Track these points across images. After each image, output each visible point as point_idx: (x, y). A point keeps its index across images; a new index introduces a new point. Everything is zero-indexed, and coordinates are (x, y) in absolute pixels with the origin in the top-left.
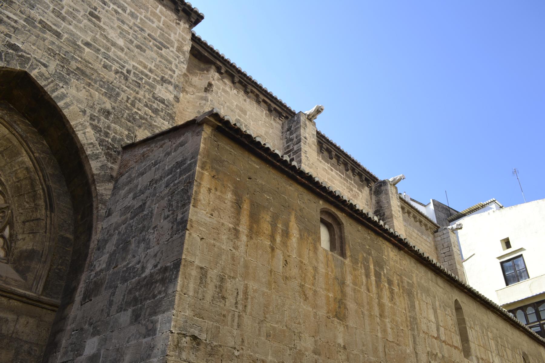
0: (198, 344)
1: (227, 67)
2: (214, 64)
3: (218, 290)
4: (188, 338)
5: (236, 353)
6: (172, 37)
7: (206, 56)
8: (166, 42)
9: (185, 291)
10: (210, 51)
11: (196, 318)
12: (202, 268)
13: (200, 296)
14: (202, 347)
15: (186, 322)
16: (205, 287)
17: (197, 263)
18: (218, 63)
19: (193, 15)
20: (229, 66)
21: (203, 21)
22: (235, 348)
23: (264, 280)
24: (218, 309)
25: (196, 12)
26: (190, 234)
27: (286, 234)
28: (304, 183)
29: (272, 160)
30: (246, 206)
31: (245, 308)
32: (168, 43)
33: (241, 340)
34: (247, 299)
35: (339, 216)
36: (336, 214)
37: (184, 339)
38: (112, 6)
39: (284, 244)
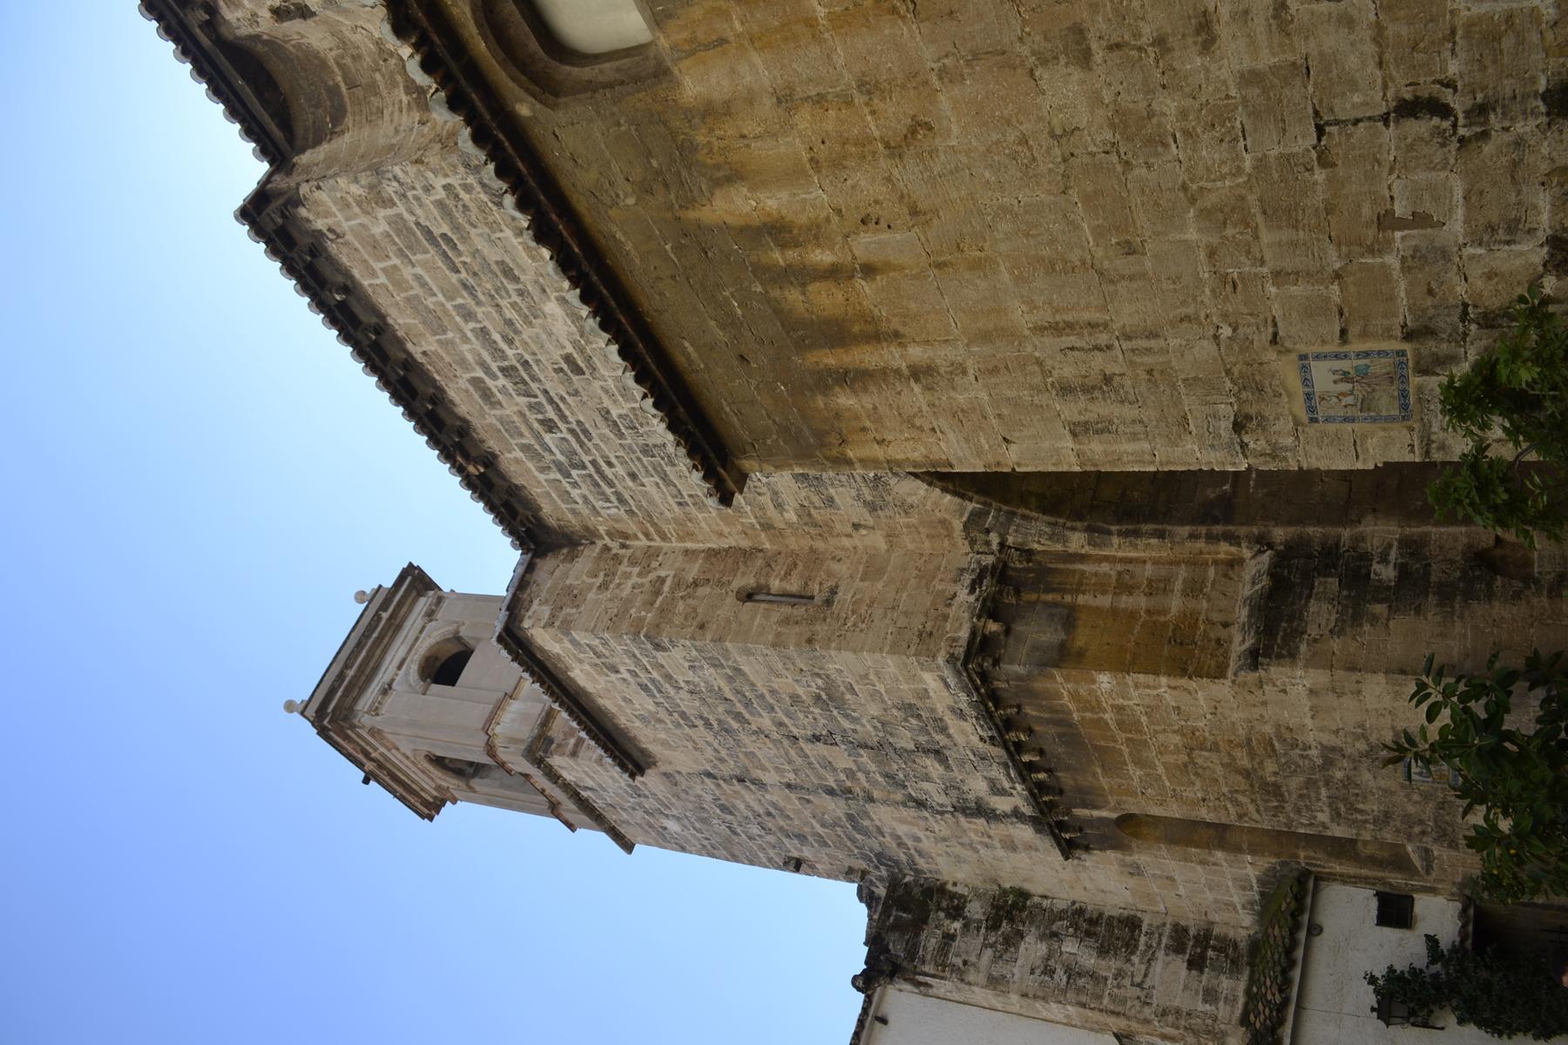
0: (1248, 418)
1: (176, 15)
2: (219, 41)
3: (1097, 394)
4: (1246, 439)
5: (1226, 331)
6: (380, 228)
7: (243, 78)
8: (417, 239)
9: (1147, 458)
10: (223, 87)
11: (1192, 427)
12: (1074, 434)
13: (1138, 428)
14: (1253, 411)
15: (1212, 446)
16: (1111, 422)
17: (1068, 443)
18: (205, 41)
19: (300, 266)
20: (169, 16)
21: (239, 203)
22: (1216, 337)
23: (982, 284)
24: (1143, 388)
25: (259, 231)
26: (1019, 465)
27: (777, 231)
28: (559, 216)
29: (636, 339)
30: (830, 359)
31: (1098, 325)
32: (409, 230)
33: (1185, 324)
34: (1070, 326)
35: (467, 10)
36: (479, 25)
37: (1252, 445)
38: (510, 352)
39: (816, 233)
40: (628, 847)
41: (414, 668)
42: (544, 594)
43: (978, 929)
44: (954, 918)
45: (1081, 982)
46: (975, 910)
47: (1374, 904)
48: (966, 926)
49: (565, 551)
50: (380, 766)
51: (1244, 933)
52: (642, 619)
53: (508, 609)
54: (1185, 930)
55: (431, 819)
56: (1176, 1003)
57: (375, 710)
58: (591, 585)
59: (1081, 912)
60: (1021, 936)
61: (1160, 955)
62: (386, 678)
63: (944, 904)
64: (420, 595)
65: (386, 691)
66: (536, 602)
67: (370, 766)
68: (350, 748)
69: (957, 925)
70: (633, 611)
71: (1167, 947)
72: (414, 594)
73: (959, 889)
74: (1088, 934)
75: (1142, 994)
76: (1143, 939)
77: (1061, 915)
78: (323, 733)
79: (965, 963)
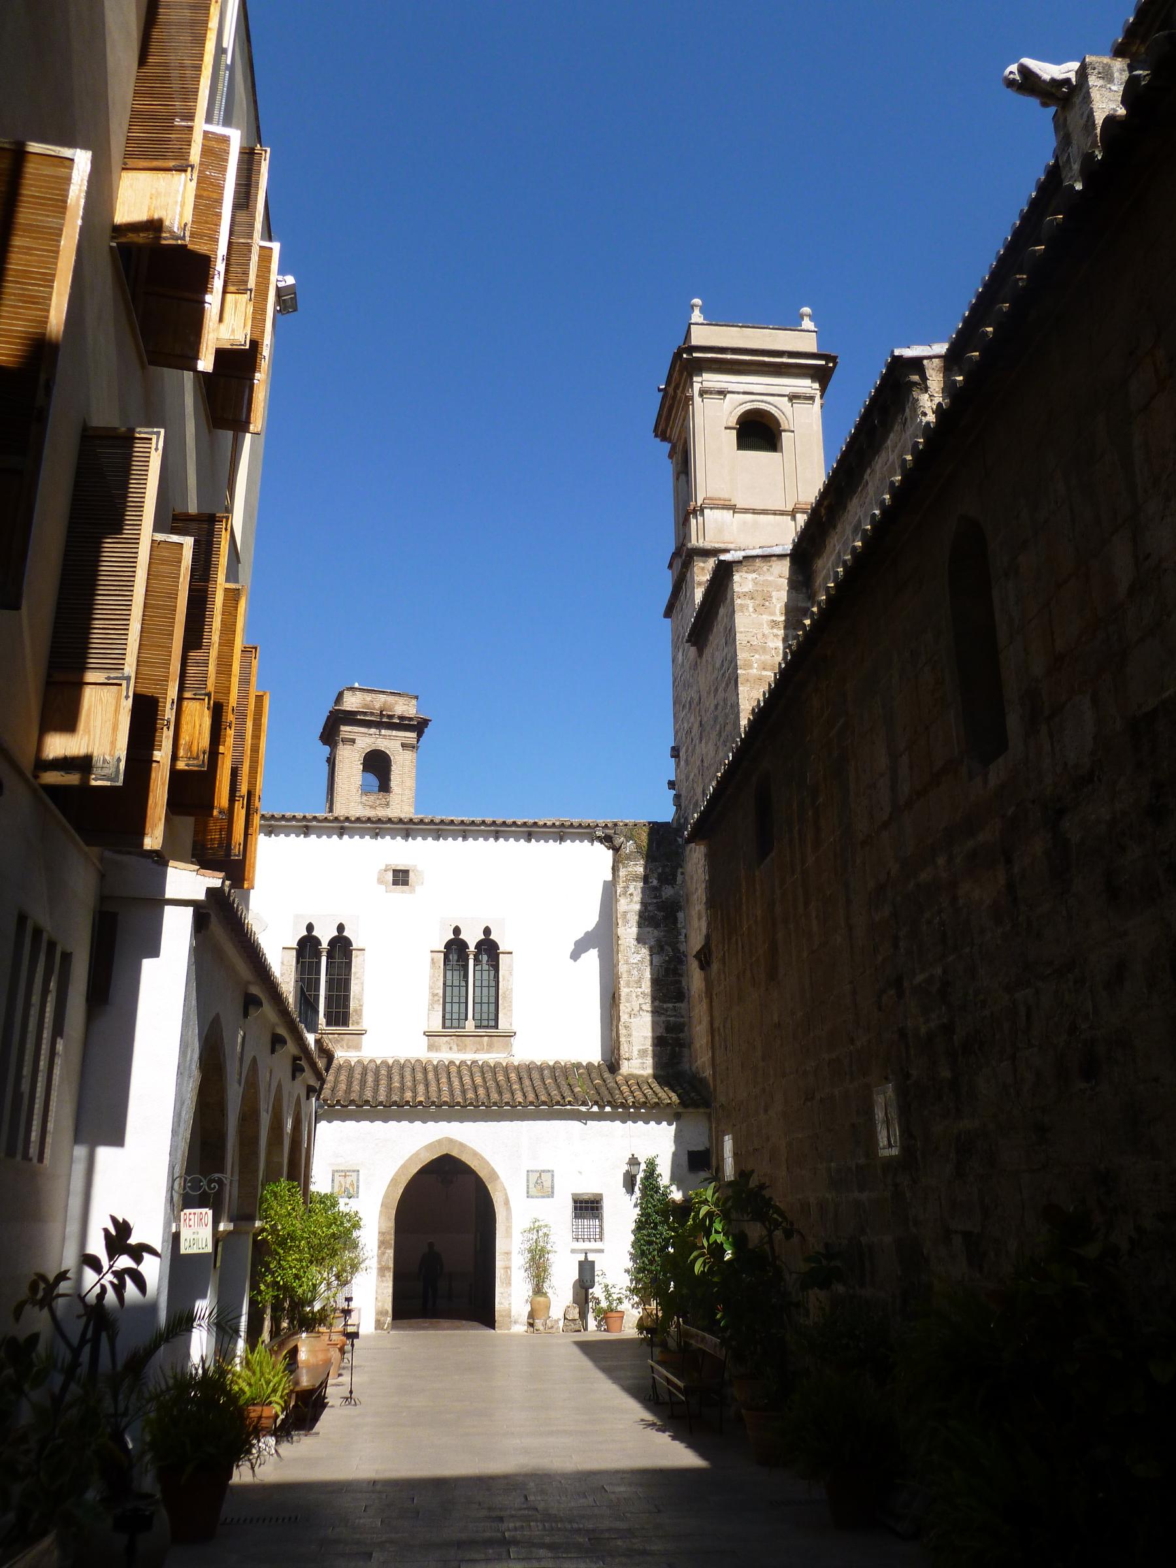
40: (668, 613)
41: (748, 406)
42: (761, 578)
43: (655, 897)
44: (659, 879)
45: (635, 972)
46: (668, 892)
47: (701, 1148)
48: (655, 889)
49: (800, 578)
50: (674, 398)
51: (687, 1067)
52: (751, 667)
53: (744, 557)
54: (682, 1031)
55: (656, 436)
56: (634, 1033)
57: (702, 393)
58: (773, 614)
59: (681, 962)
60: (657, 926)
61: (663, 1018)
62: (731, 387)
63: (667, 870)
64: (814, 378)
65: (723, 393)
66: (754, 575)
67: (671, 391)
68: (676, 374)
69: (655, 882)
70: (757, 656)
71: (668, 1022)
72: (811, 372)
73: (679, 878)
74: (667, 970)
75: (635, 1011)
76: (670, 1005)
77: (676, 950)
78: (677, 356)
79: (631, 895)
